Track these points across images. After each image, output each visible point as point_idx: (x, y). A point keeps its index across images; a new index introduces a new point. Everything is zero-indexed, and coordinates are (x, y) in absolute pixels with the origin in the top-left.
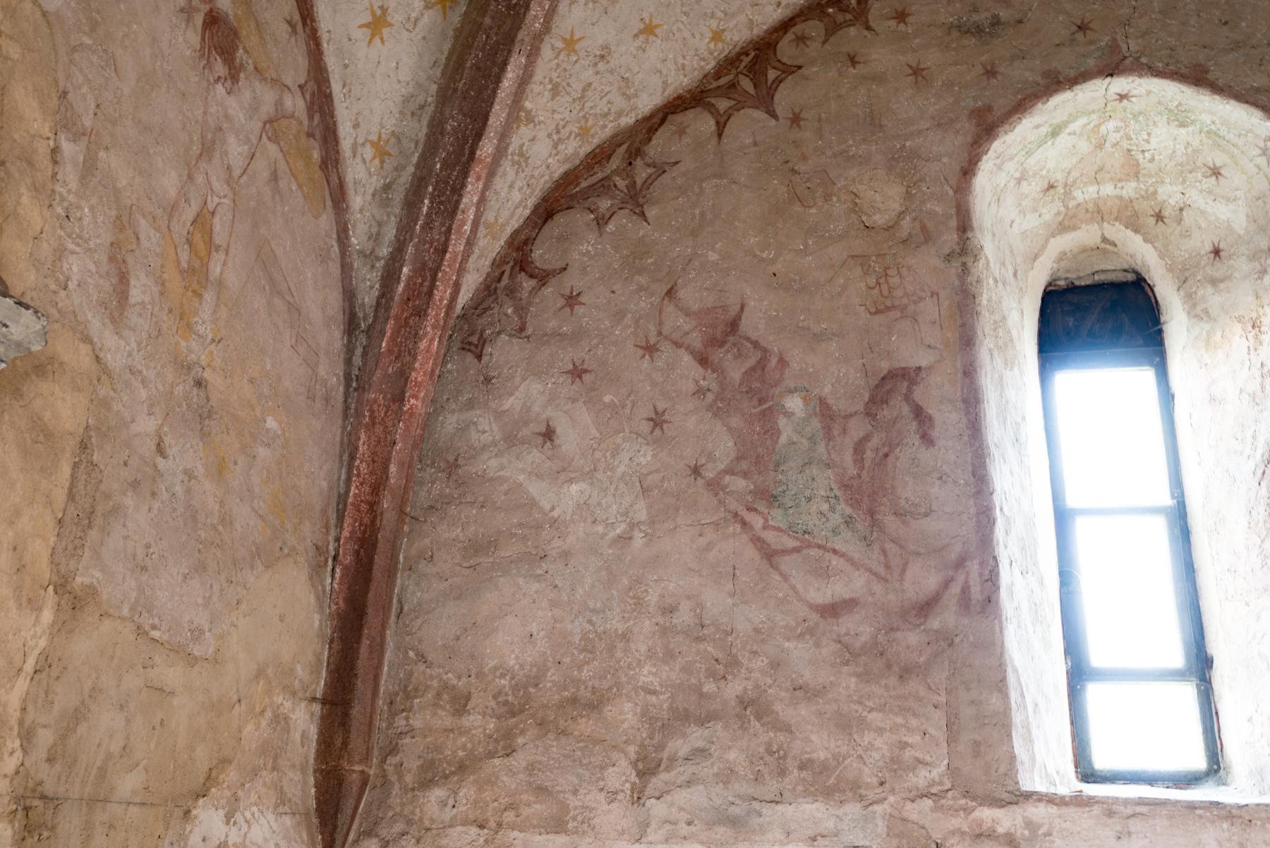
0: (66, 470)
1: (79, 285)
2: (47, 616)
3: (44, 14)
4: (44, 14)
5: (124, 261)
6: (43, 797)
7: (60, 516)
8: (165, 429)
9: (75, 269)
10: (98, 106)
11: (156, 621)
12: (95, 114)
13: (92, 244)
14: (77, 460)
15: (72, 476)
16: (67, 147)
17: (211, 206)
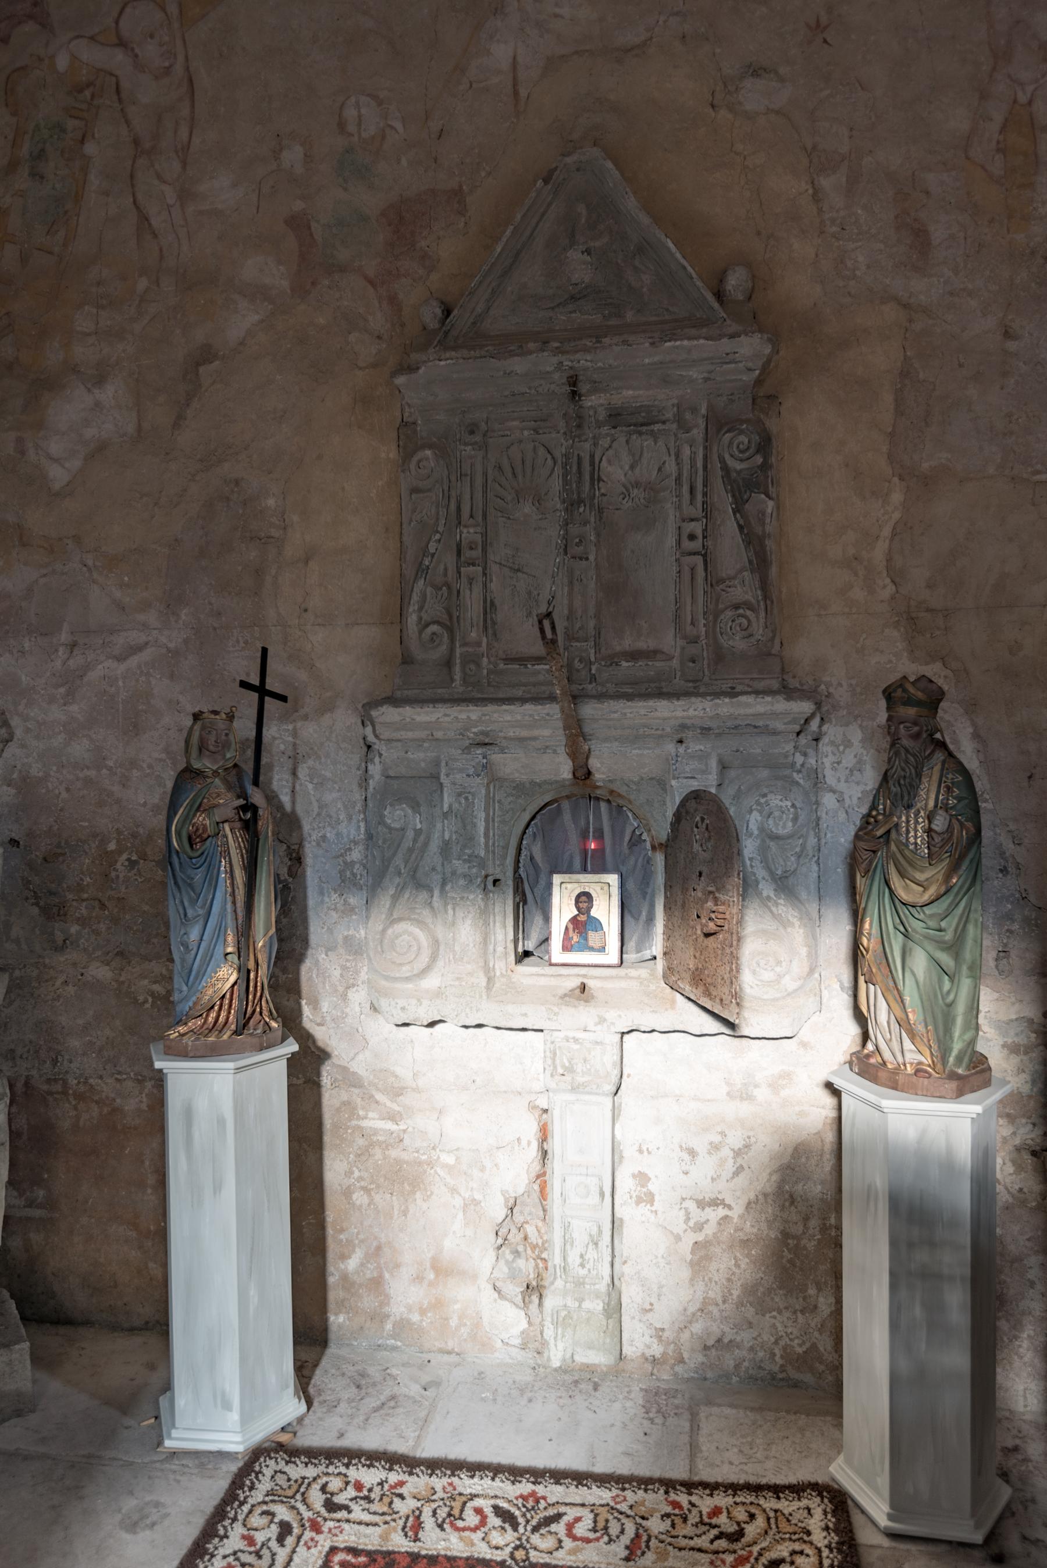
0: (888, 398)
1: (868, 267)
2: (897, 497)
3: (778, 112)
4: (778, 112)
5: (915, 220)
6: (928, 610)
7: (890, 430)
8: (1010, 317)
9: (861, 259)
10: (851, 129)
11: (1039, 467)
12: (851, 137)
13: (873, 231)
14: (899, 386)
15: (896, 400)
16: (825, 183)
17: (1022, 98)
